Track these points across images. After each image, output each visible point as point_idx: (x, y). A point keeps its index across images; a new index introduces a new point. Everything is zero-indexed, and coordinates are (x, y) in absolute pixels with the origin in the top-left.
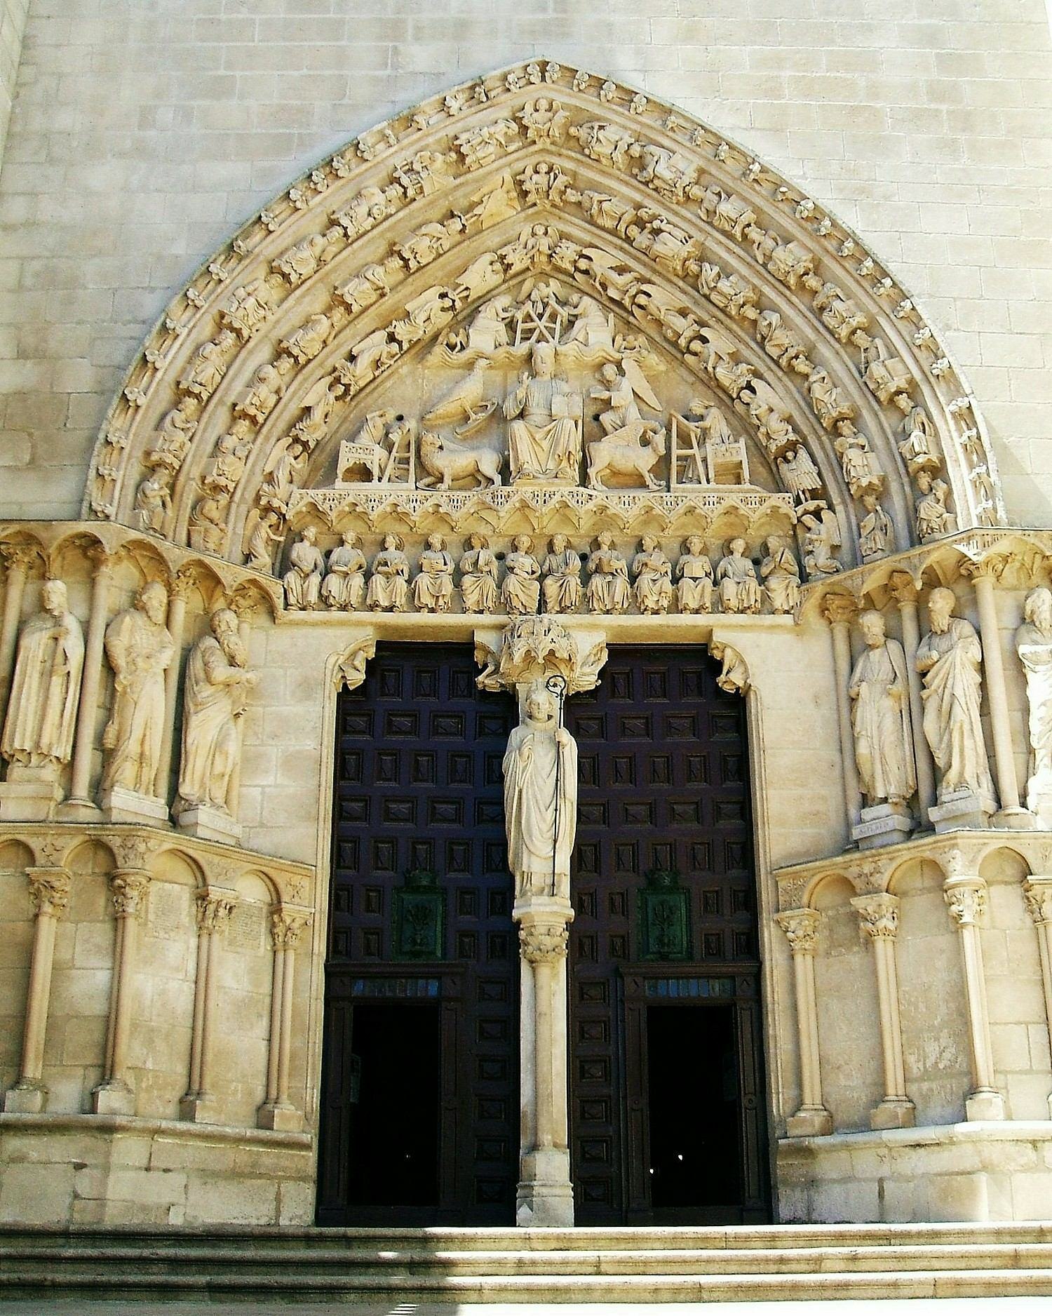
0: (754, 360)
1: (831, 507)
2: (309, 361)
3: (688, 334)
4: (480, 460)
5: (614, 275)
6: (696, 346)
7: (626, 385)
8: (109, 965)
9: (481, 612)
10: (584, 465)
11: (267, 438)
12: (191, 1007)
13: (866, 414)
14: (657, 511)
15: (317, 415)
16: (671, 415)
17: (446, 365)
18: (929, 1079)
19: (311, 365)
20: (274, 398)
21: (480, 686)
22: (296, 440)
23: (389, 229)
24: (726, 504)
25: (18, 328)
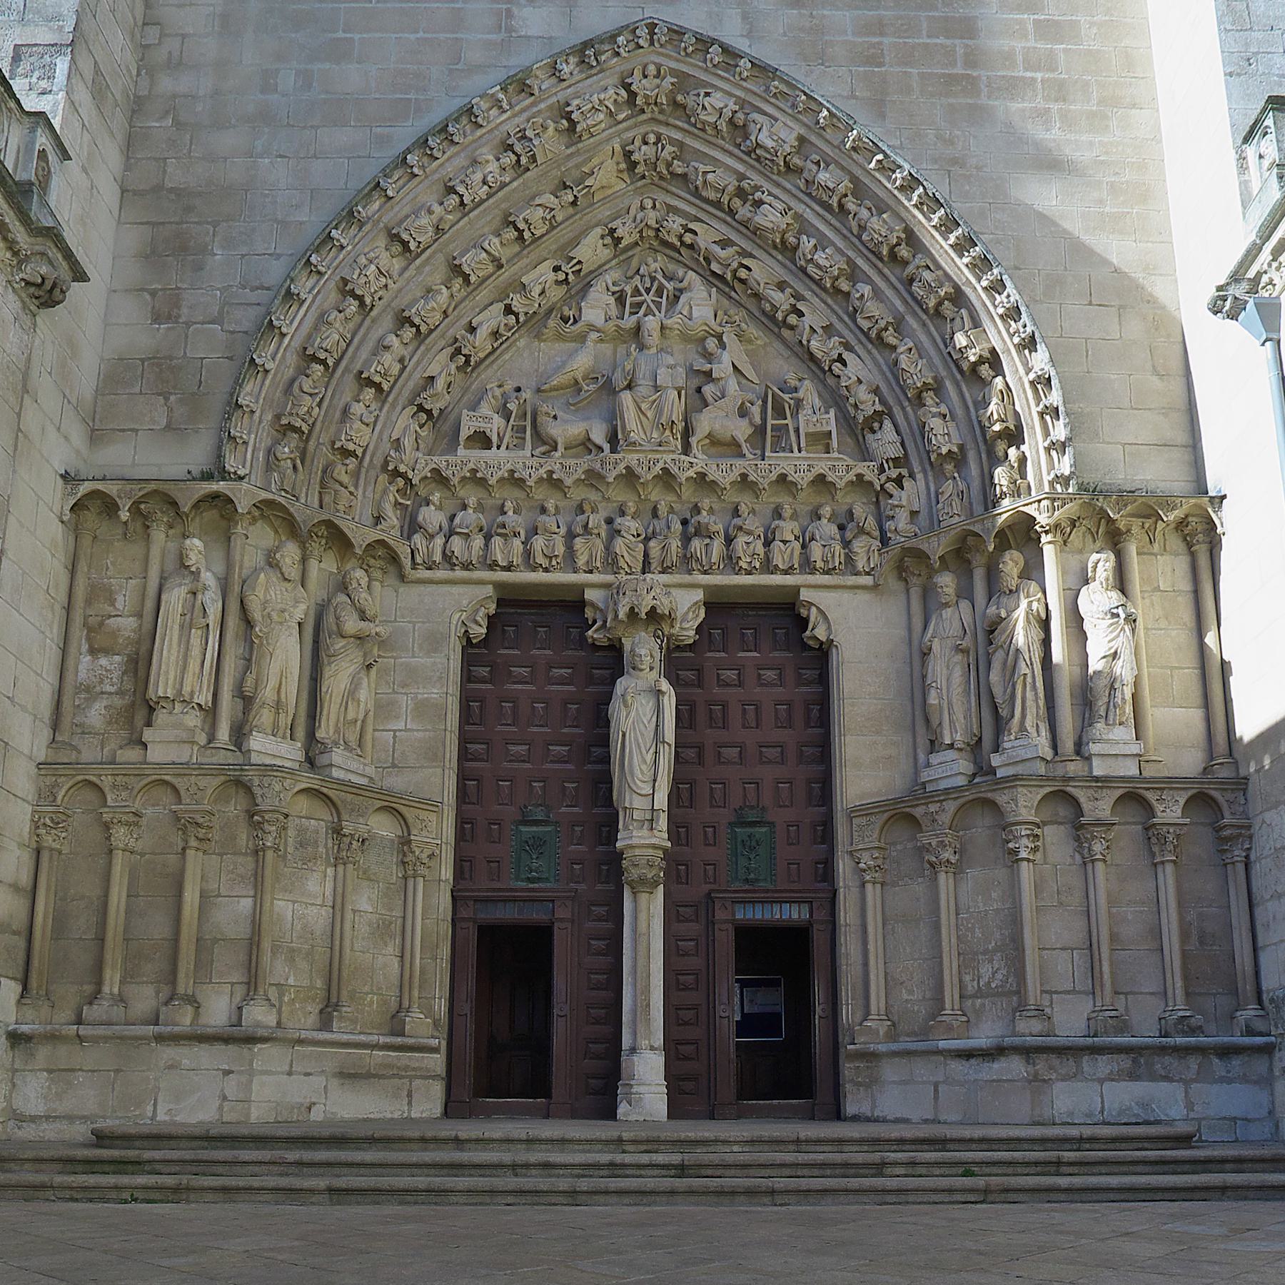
0: (846, 333)
1: (912, 476)
2: (431, 331)
3: (786, 307)
4: (591, 429)
5: (717, 249)
6: (792, 319)
7: (726, 357)
8: (252, 893)
9: (591, 572)
10: (687, 433)
11: (393, 406)
12: (329, 929)
13: (948, 384)
14: (751, 478)
15: (440, 384)
16: (767, 386)
17: (560, 337)
18: (981, 997)
19: (434, 335)
20: (396, 368)
21: (590, 640)
22: (421, 408)
23: (505, 199)
24: (818, 470)
25: (153, 293)
